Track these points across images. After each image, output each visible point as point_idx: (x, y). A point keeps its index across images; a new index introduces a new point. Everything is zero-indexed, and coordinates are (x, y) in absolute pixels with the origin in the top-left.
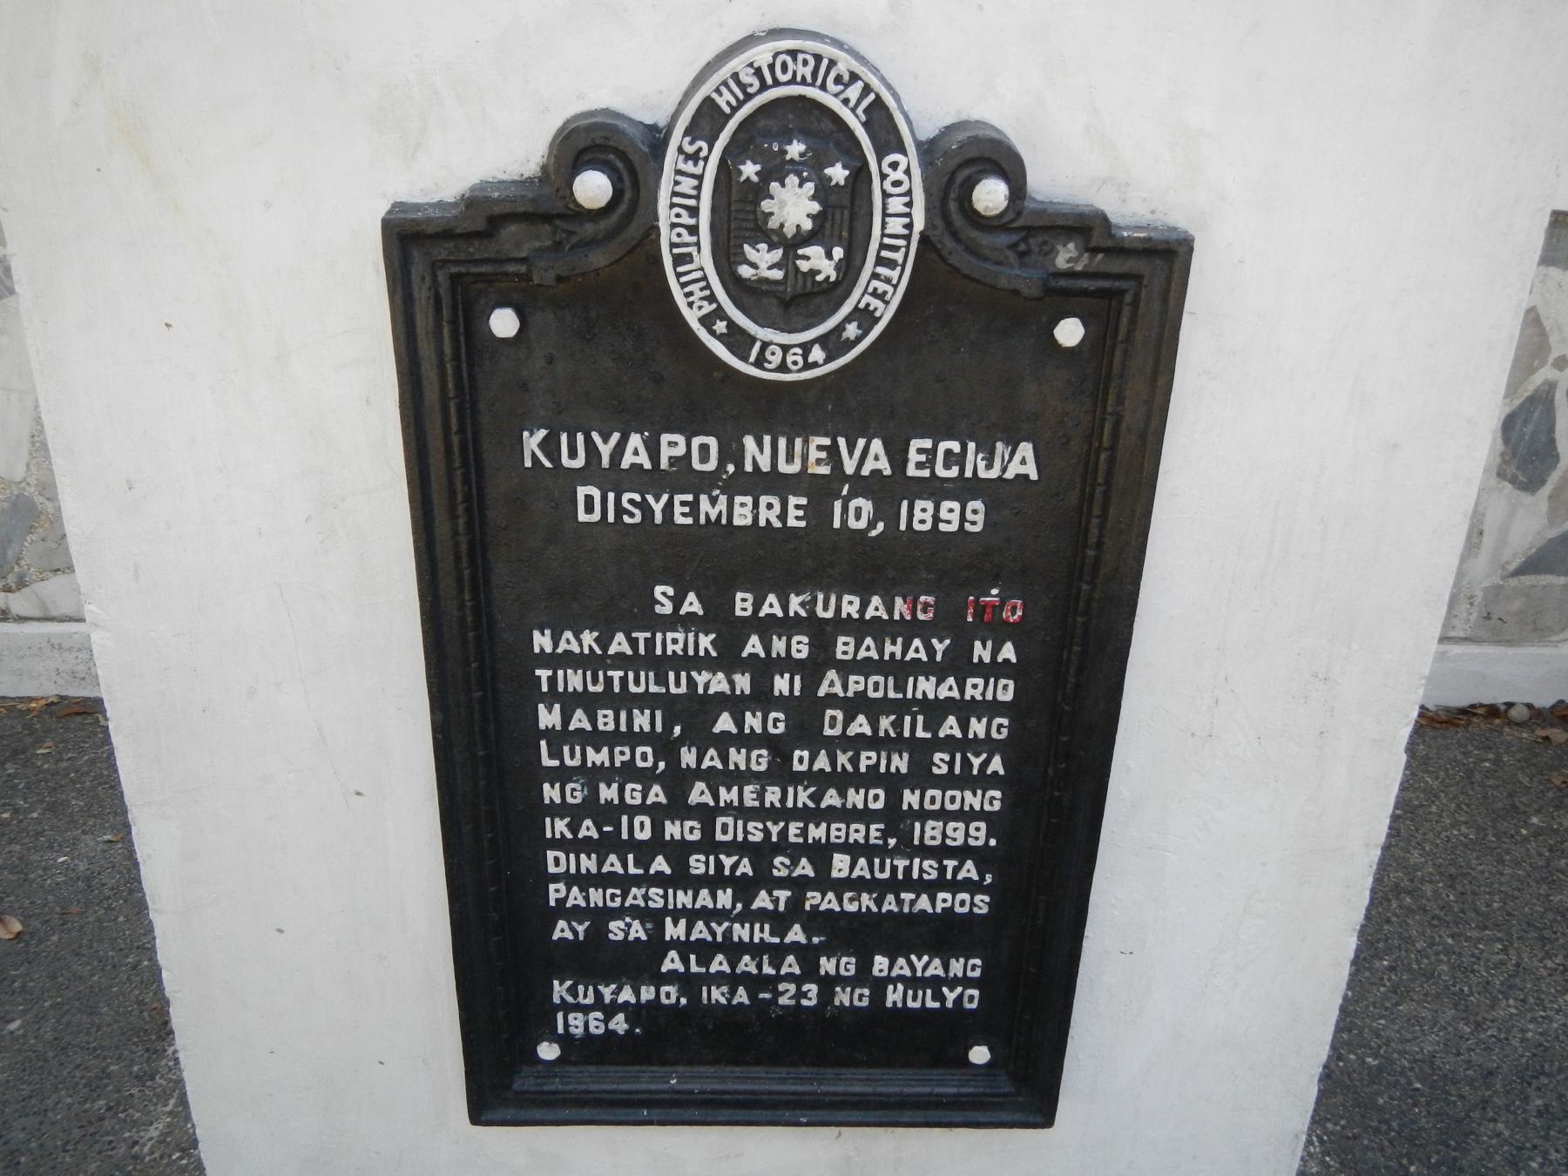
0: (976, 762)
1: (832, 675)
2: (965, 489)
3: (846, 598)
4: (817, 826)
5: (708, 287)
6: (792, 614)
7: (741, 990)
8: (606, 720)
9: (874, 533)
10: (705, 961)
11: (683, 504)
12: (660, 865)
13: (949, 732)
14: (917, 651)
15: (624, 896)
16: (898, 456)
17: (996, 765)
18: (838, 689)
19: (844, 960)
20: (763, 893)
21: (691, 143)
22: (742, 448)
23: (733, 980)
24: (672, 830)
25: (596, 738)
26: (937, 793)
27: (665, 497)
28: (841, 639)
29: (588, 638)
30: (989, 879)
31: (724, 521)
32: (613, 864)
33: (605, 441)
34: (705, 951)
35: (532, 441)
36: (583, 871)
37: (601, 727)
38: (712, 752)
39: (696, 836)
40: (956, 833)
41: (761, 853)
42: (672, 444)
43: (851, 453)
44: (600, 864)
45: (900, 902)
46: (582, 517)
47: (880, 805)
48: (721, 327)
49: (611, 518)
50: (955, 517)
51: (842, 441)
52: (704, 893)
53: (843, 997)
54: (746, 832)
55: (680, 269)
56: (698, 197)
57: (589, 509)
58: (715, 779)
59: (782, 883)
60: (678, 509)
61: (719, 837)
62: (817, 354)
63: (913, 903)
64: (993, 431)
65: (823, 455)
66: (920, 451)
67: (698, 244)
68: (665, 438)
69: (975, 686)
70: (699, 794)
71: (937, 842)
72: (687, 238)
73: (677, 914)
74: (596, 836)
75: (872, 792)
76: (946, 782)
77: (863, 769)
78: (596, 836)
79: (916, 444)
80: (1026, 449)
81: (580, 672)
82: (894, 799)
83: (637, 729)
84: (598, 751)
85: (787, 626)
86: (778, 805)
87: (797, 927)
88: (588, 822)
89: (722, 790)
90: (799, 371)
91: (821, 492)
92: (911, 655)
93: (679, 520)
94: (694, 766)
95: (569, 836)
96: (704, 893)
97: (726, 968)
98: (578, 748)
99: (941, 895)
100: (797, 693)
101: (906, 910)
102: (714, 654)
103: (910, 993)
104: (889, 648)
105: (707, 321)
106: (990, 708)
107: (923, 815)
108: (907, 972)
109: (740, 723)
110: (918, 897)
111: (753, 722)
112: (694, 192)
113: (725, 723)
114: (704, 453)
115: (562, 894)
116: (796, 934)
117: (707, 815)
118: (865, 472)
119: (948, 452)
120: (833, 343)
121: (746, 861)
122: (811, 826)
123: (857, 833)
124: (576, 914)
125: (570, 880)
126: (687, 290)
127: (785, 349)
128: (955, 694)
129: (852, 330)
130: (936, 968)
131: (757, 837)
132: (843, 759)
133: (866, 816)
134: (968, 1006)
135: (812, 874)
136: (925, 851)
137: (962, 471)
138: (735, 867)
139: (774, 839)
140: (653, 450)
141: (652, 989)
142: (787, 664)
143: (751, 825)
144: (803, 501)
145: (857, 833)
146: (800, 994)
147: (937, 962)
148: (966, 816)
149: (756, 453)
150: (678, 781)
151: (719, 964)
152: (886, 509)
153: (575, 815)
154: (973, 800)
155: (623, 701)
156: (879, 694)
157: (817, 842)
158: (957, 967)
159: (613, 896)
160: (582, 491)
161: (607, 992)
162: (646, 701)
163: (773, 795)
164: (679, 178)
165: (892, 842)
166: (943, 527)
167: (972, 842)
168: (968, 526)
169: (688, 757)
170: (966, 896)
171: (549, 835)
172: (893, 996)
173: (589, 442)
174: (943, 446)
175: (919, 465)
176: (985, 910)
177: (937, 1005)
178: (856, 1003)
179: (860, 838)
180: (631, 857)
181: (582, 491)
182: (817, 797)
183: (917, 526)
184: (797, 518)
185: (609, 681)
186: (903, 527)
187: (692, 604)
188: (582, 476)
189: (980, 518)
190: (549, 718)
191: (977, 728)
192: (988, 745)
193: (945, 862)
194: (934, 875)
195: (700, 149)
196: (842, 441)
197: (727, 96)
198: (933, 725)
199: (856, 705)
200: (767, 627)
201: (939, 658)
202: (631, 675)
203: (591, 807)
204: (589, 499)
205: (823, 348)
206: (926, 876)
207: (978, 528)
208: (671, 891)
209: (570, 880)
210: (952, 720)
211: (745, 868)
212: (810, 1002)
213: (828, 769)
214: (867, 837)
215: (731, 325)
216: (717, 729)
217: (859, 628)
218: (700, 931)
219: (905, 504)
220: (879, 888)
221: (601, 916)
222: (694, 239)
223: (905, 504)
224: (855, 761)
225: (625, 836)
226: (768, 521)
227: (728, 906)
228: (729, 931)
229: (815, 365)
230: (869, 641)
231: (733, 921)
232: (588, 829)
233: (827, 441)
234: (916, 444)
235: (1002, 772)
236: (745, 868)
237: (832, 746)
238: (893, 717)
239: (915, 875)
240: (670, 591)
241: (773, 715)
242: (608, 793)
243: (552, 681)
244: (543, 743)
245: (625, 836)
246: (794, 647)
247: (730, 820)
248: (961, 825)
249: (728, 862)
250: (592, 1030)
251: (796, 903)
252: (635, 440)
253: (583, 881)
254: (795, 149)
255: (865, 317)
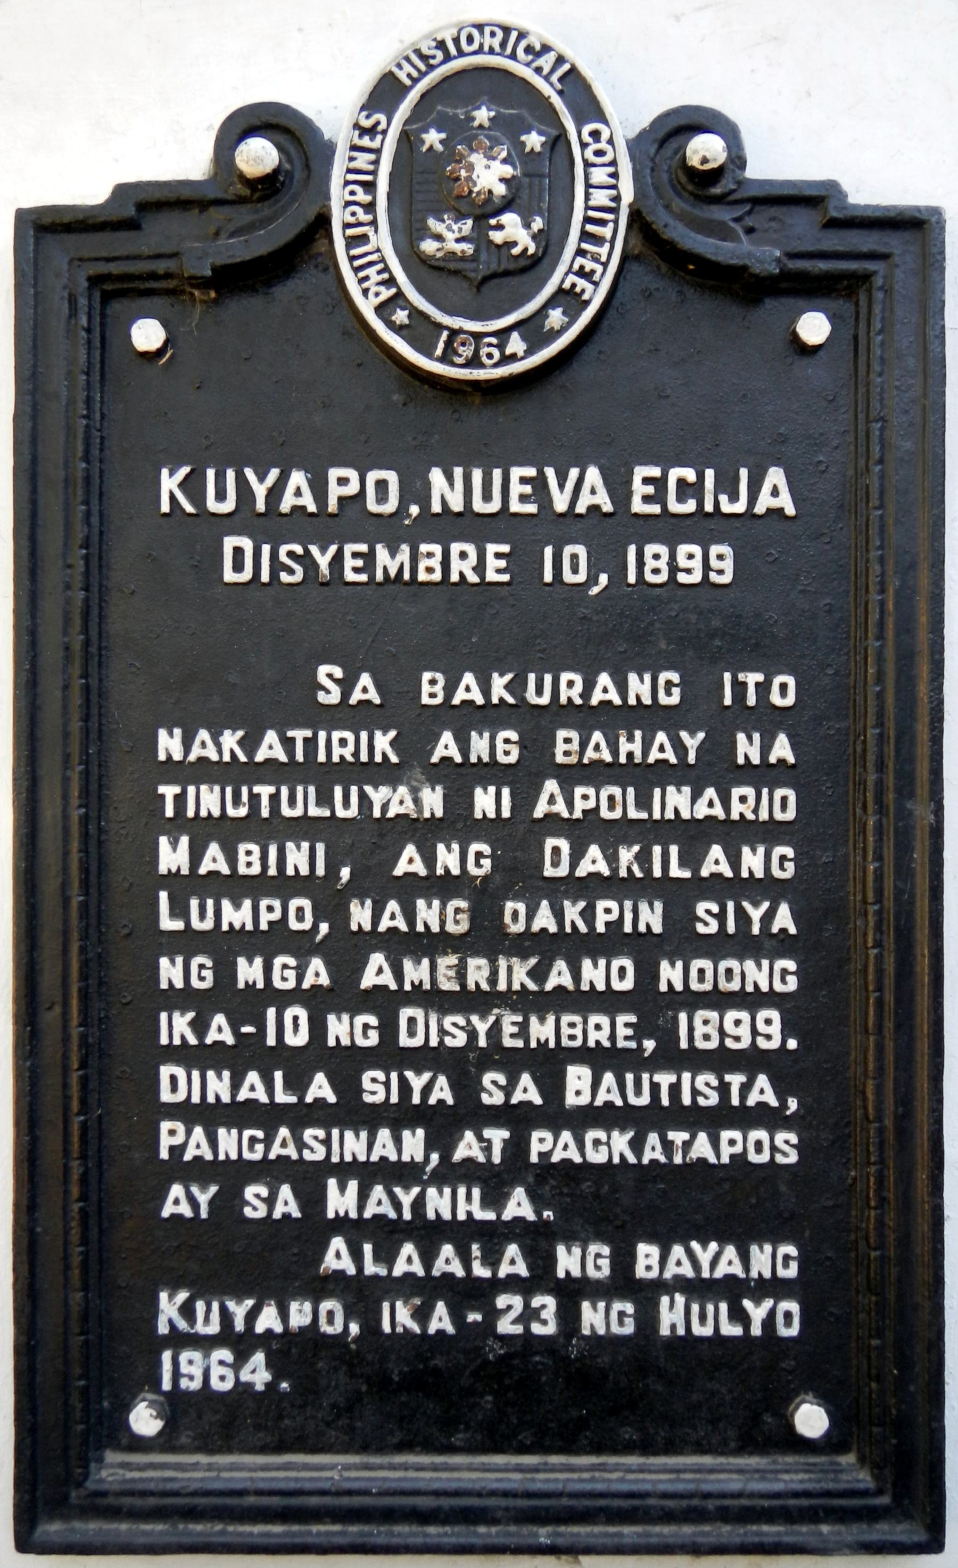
0: (756, 914)
1: (551, 786)
2: (705, 527)
3: (565, 677)
4: (542, 1020)
5: (386, 269)
6: (495, 700)
7: (441, 1308)
8: (249, 857)
9: (595, 590)
10: (386, 1255)
11: (355, 555)
12: (321, 1088)
13: (715, 869)
14: (662, 749)
15: (268, 1142)
16: (619, 487)
17: (784, 919)
18: (560, 808)
19: (593, 1248)
20: (469, 1135)
21: (368, 117)
22: (427, 485)
23: (426, 1289)
24: (338, 1029)
25: (235, 886)
26: (707, 964)
27: (333, 549)
28: (561, 734)
29: (230, 740)
30: (793, 1104)
31: (407, 576)
32: (253, 1087)
33: (261, 479)
34: (386, 1234)
35: (169, 483)
36: (211, 1099)
37: (242, 870)
38: (393, 906)
39: (373, 1039)
40: (738, 1028)
41: (462, 1066)
42: (343, 481)
43: (561, 486)
44: (236, 1086)
45: (668, 1146)
46: (229, 576)
47: (628, 984)
48: (401, 316)
49: (265, 577)
50: (697, 564)
51: (550, 472)
52: (384, 1134)
53: (592, 1317)
54: (442, 1032)
55: (355, 252)
56: (374, 173)
57: (238, 567)
58: (403, 945)
59: (497, 1115)
60: (349, 563)
61: (405, 1041)
62: (516, 344)
63: (687, 1145)
64: (733, 456)
65: (528, 489)
66: (646, 481)
67: (374, 223)
68: (334, 473)
69: (743, 799)
70: (375, 972)
71: (713, 1044)
72: (363, 216)
73: (345, 1170)
74: (230, 1040)
75: (616, 964)
76: (717, 947)
77: (600, 928)
78: (230, 1040)
79: (641, 472)
80: (775, 476)
81: (217, 789)
82: (647, 975)
83: (290, 871)
84: (237, 906)
85: (488, 716)
86: (485, 986)
87: (519, 1193)
88: (220, 1019)
89: (408, 965)
90: (496, 365)
91: (528, 534)
92: (654, 755)
93: (350, 576)
94: (367, 927)
95: (192, 1040)
96: (384, 1134)
97: (418, 1268)
98: (210, 903)
99: (726, 1135)
100: (506, 814)
101: (678, 1159)
102: (394, 759)
103: (695, 1308)
104: (625, 747)
105: (382, 310)
106: (767, 833)
107: (692, 1000)
108: (687, 1271)
109: (430, 859)
110: (693, 1137)
111: (448, 858)
112: (371, 167)
113: (409, 861)
114: (381, 486)
115: (179, 1140)
116: (519, 1205)
117: (385, 1003)
118: (581, 508)
119: (681, 482)
120: (535, 332)
121: (442, 1081)
122: (534, 1020)
123: (598, 1029)
124: (199, 1171)
125: (189, 1113)
126: (362, 274)
127: (478, 336)
128: (718, 811)
129: (556, 317)
130: (729, 1264)
131: (460, 1040)
132: (573, 912)
133: (608, 1001)
134: (784, 1332)
135: (538, 1101)
136: (696, 1060)
137: (700, 504)
138: (427, 1090)
139: (482, 1043)
140: (319, 489)
141: (308, 1306)
142: (491, 772)
143: (448, 1021)
144: (505, 548)
145: (598, 1029)
146: (530, 1315)
147: (730, 1252)
148: (752, 1000)
149: (445, 490)
150: (347, 951)
151: (407, 1259)
152: (607, 557)
153: (200, 1004)
154: (757, 974)
155: (271, 829)
156: (617, 814)
157: (542, 1045)
158: (762, 1260)
159: (253, 1140)
160: (230, 542)
161: (239, 1310)
162: (304, 828)
163: (478, 971)
164: (355, 154)
165: (649, 1045)
166: (682, 578)
167: (762, 1044)
168: (714, 577)
169: (360, 915)
170: (760, 1134)
171: (164, 1040)
172: (671, 1315)
173: (241, 481)
174: (675, 474)
175: (647, 499)
176: (793, 1158)
177: (737, 1331)
178: (616, 1329)
179: (603, 1037)
180: (278, 1076)
181: (230, 542)
182: (539, 974)
183: (650, 578)
184: (499, 571)
185: (255, 799)
186: (632, 579)
187: (366, 688)
188: (230, 524)
189: (728, 565)
190: (172, 857)
191: (752, 861)
192: (767, 888)
193: (728, 1078)
194: (713, 1099)
195: (378, 123)
196: (550, 472)
197: (408, 68)
198: (692, 859)
199: (585, 830)
200: (466, 719)
201: (692, 758)
202: (285, 791)
203: (226, 996)
204: (238, 552)
205: (524, 338)
206: (701, 1101)
207: (727, 579)
208: (335, 1132)
209: (189, 1113)
210: (716, 851)
211: (443, 1092)
212: (546, 1327)
213: (553, 929)
214: (613, 1037)
215: (416, 313)
216: (401, 869)
217: (586, 716)
218: (379, 1203)
219: (632, 550)
220: (638, 1121)
221: (232, 1176)
222: (369, 218)
223: (632, 550)
224: (588, 914)
225: (271, 1041)
226: (461, 574)
227: (419, 1158)
228: (419, 1204)
229: (513, 358)
230: (597, 736)
231: (425, 1185)
232: (220, 1030)
233: (531, 472)
234: (641, 472)
235: (793, 930)
236: (443, 1092)
237: (559, 890)
238: (636, 848)
239: (686, 1100)
240: (338, 672)
241: (474, 847)
242: (249, 972)
243: (180, 800)
244: (163, 896)
245: (271, 1041)
246: (500, 747)
247: (418, 1013)
248: (744, 1016)
249: (417, 1082)
250: (216, 1384)
251: (517, 1147)
252: (298, 478)
253: (208, 1115)
254: (483, 115)
255: (569, 299)
